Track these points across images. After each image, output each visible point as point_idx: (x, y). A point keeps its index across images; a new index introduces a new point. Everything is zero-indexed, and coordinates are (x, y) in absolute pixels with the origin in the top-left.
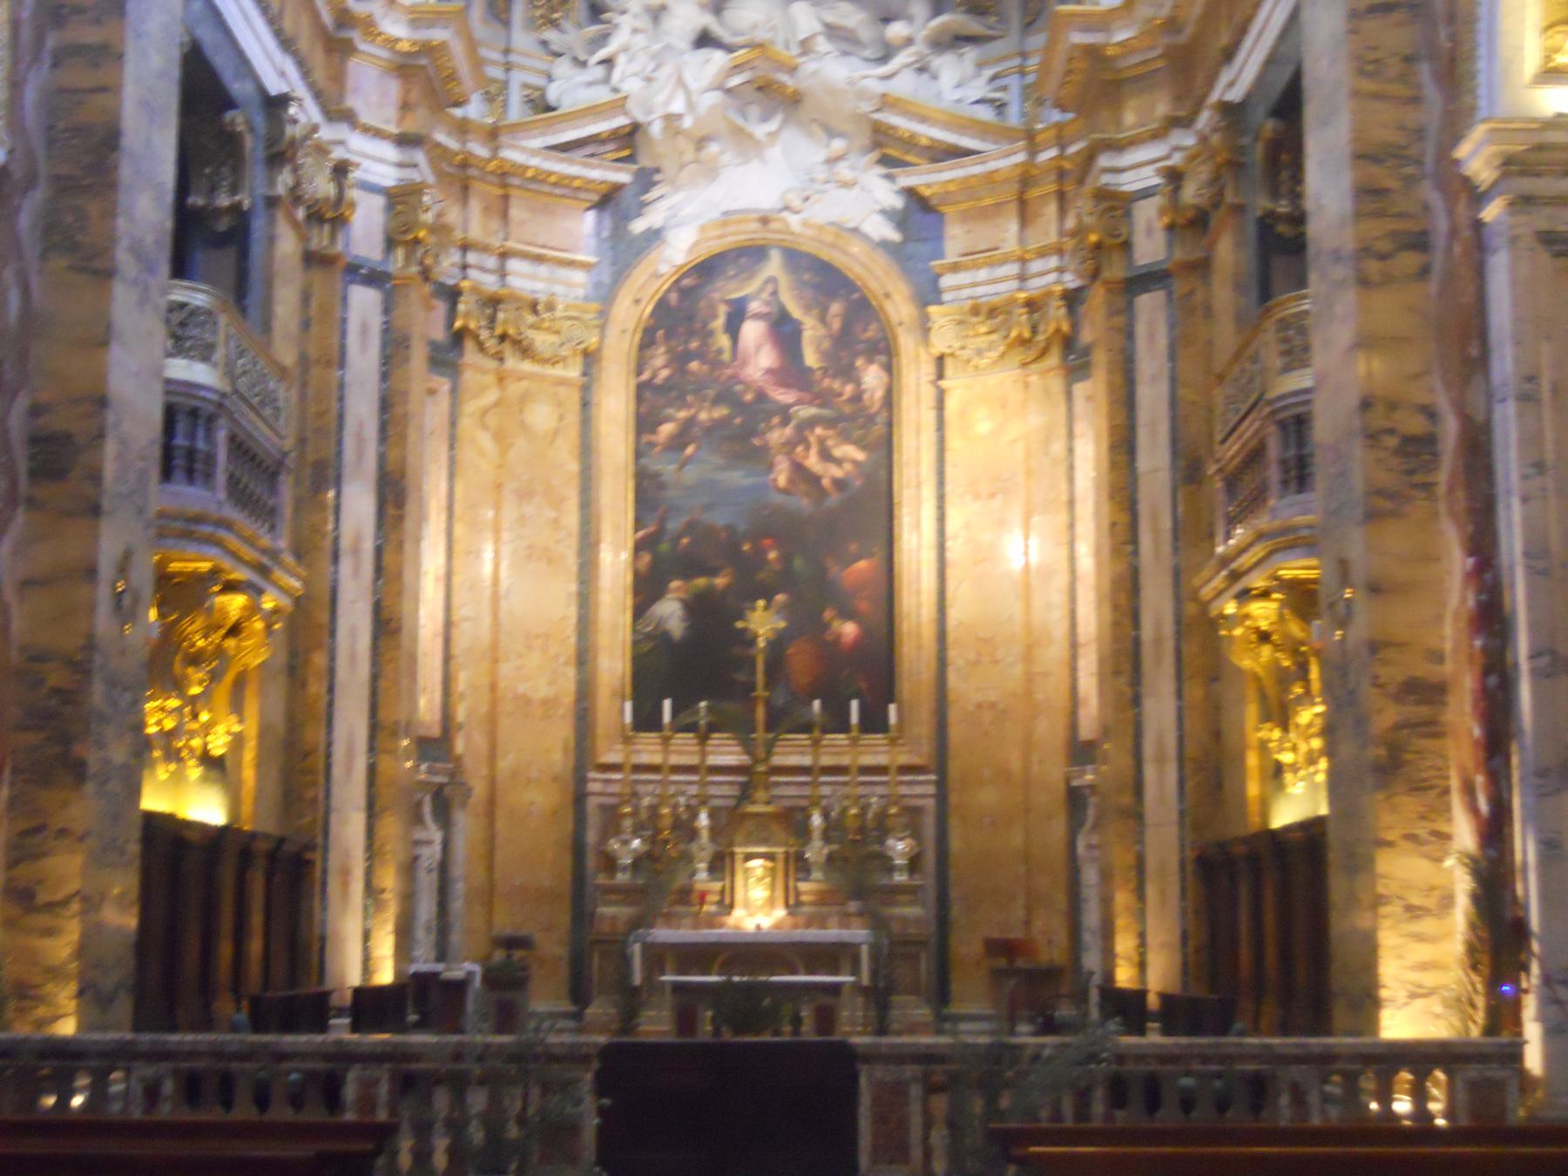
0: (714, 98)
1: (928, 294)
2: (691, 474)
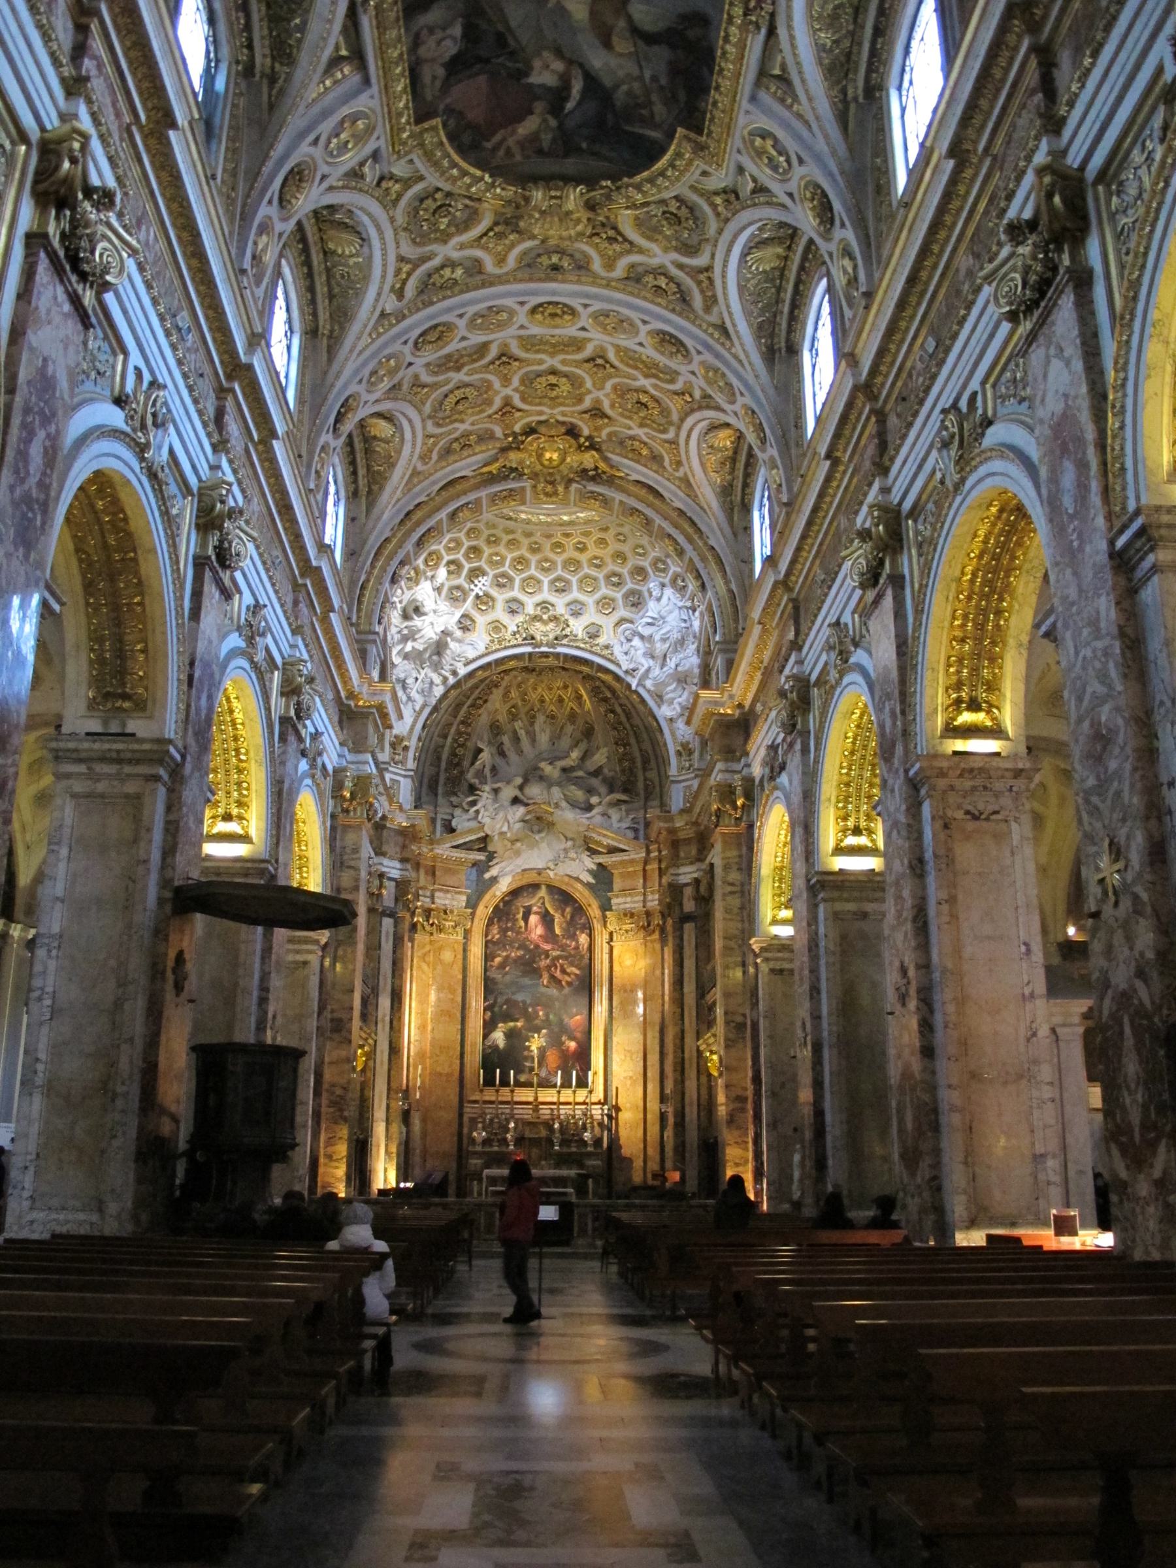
0: (519, 825)
1: (606, 907)
2: (508, 978)
